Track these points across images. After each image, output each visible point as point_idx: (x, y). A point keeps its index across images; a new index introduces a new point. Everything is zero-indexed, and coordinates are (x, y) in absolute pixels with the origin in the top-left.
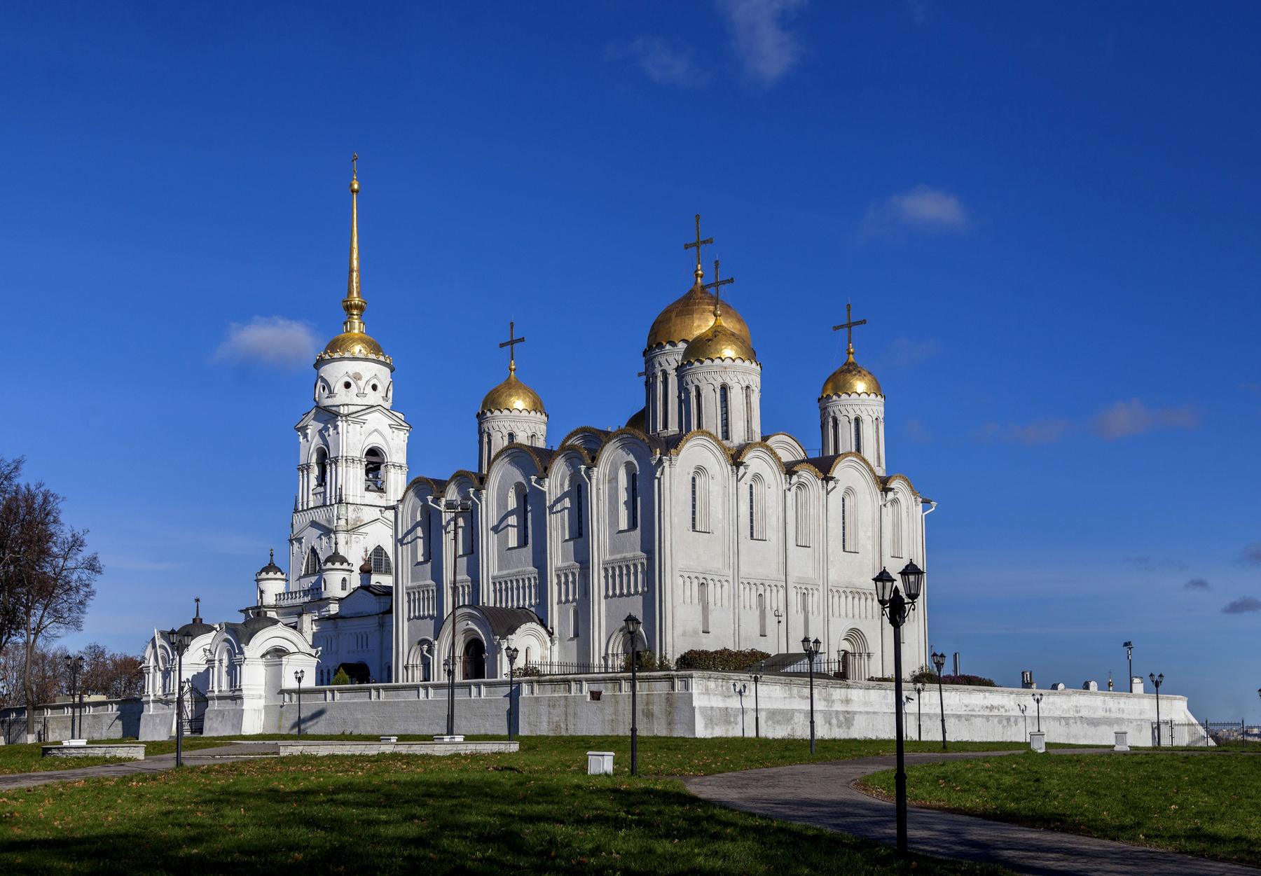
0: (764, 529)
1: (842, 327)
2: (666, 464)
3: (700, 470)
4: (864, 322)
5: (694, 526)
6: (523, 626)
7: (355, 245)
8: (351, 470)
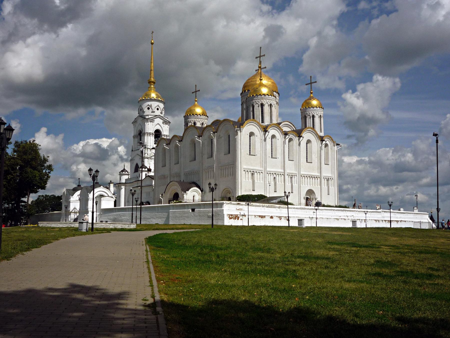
0: (276, 155)
2: (239, 132)
3: (251, 134)
5: (250, 153)
6: (192, 189)
8: (149, 137)
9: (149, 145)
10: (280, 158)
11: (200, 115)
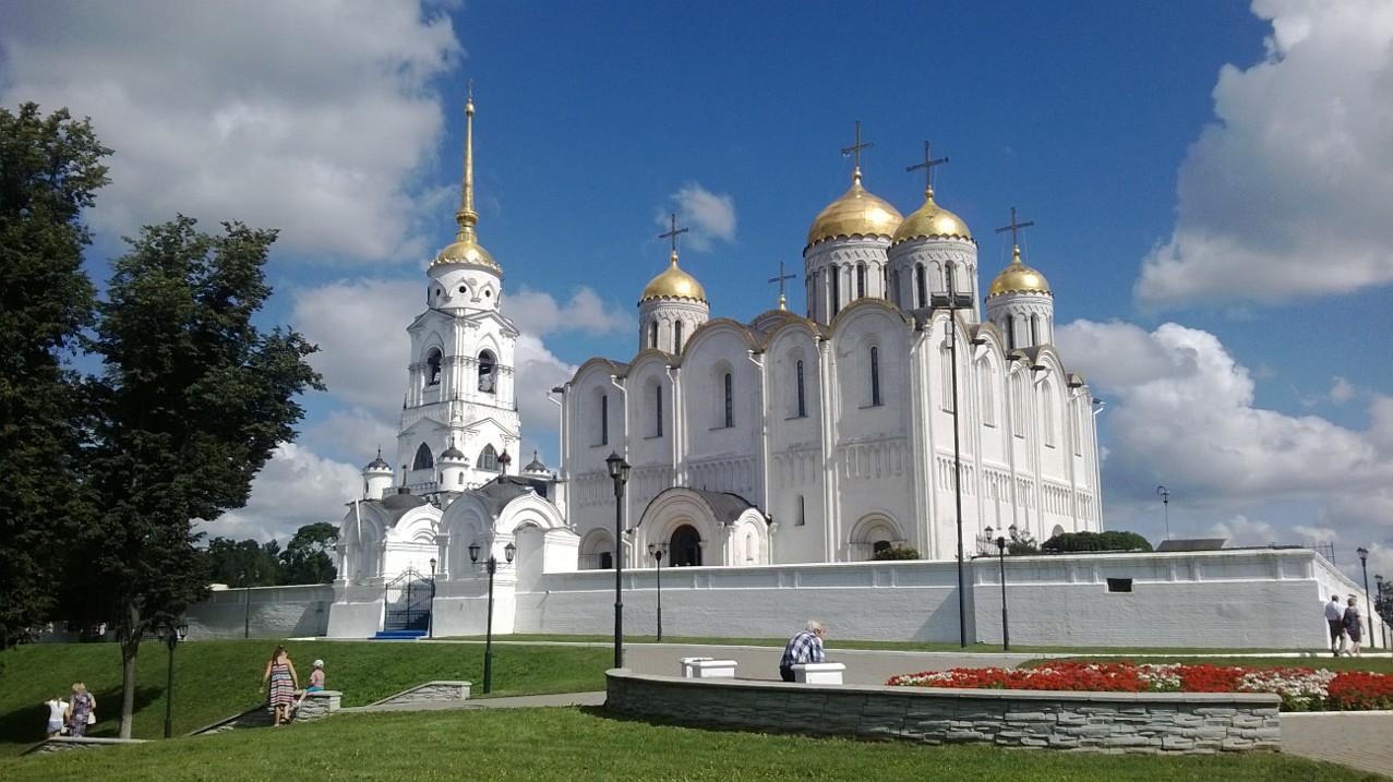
7: (470, 161)
9: (464, 390)
10: (1000, 427)
11: (694, 298)
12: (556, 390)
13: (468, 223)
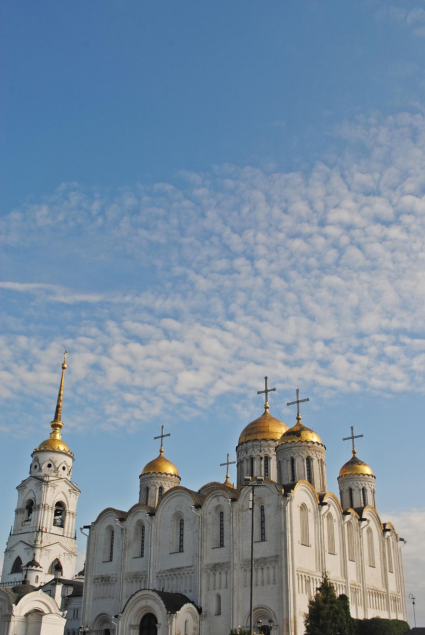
1: (348, 438)
3: (303, 507)
4: (362, 436)
10: (339, 554)
12: (85, 527)
13: (58, 428)
